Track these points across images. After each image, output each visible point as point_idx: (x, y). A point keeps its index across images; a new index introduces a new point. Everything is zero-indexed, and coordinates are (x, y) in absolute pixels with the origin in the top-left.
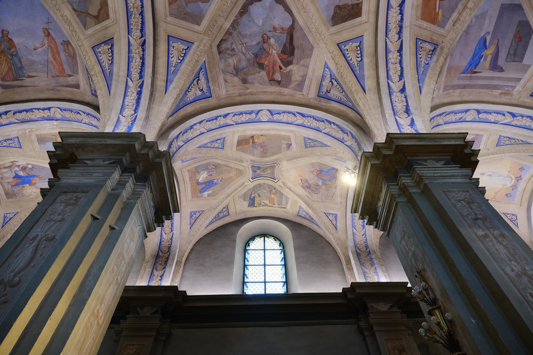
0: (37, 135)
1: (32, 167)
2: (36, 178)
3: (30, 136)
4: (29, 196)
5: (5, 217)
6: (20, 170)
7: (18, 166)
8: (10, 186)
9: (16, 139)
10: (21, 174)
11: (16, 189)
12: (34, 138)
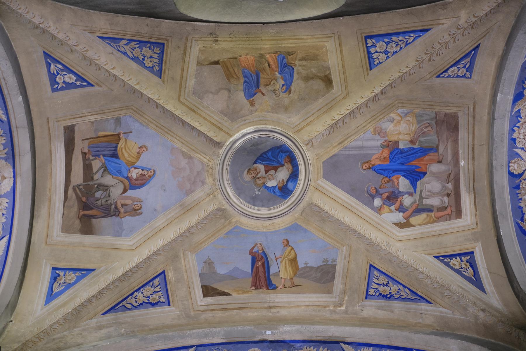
0: (330, 291)
1: (373, 197)
2: (378, 162)
3: (344, 293)
4: (406, 115)
5: (470, 69)
6: (403, 194)
7: (401, 209)
8: (441, 149)
9: (371, 292)
10: (403, 183)
11: (431, 138)
12: (338, 284)
